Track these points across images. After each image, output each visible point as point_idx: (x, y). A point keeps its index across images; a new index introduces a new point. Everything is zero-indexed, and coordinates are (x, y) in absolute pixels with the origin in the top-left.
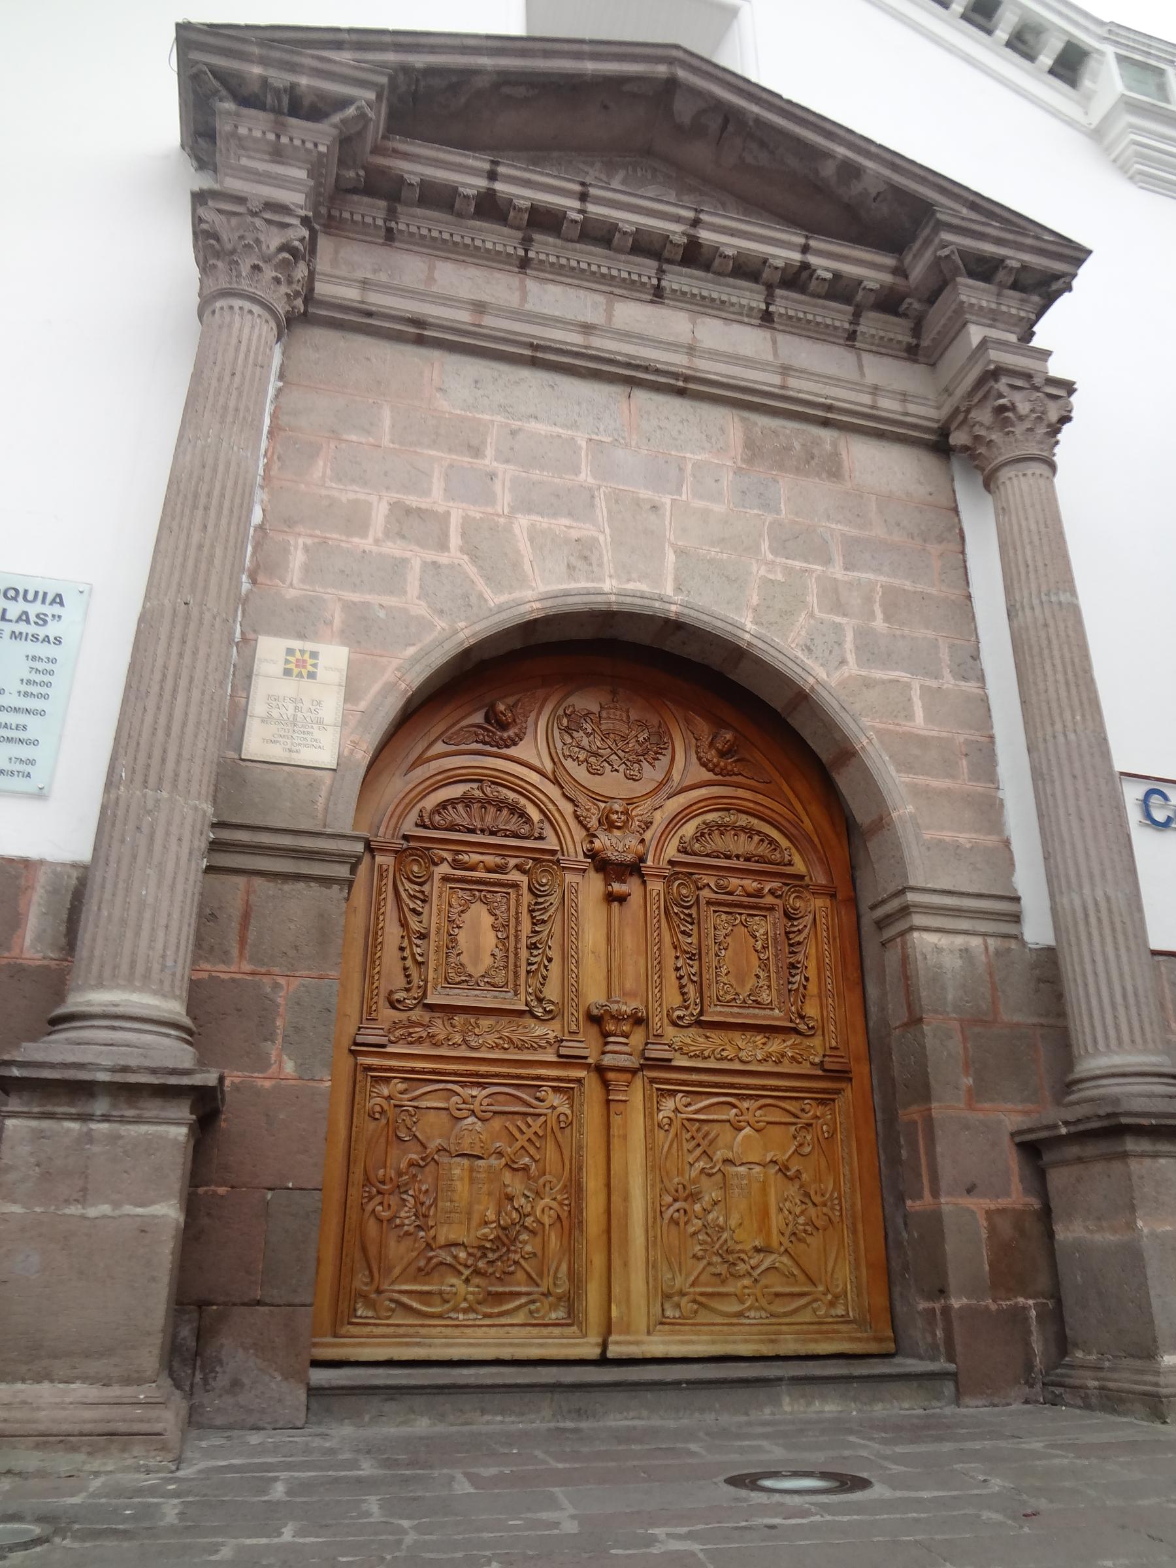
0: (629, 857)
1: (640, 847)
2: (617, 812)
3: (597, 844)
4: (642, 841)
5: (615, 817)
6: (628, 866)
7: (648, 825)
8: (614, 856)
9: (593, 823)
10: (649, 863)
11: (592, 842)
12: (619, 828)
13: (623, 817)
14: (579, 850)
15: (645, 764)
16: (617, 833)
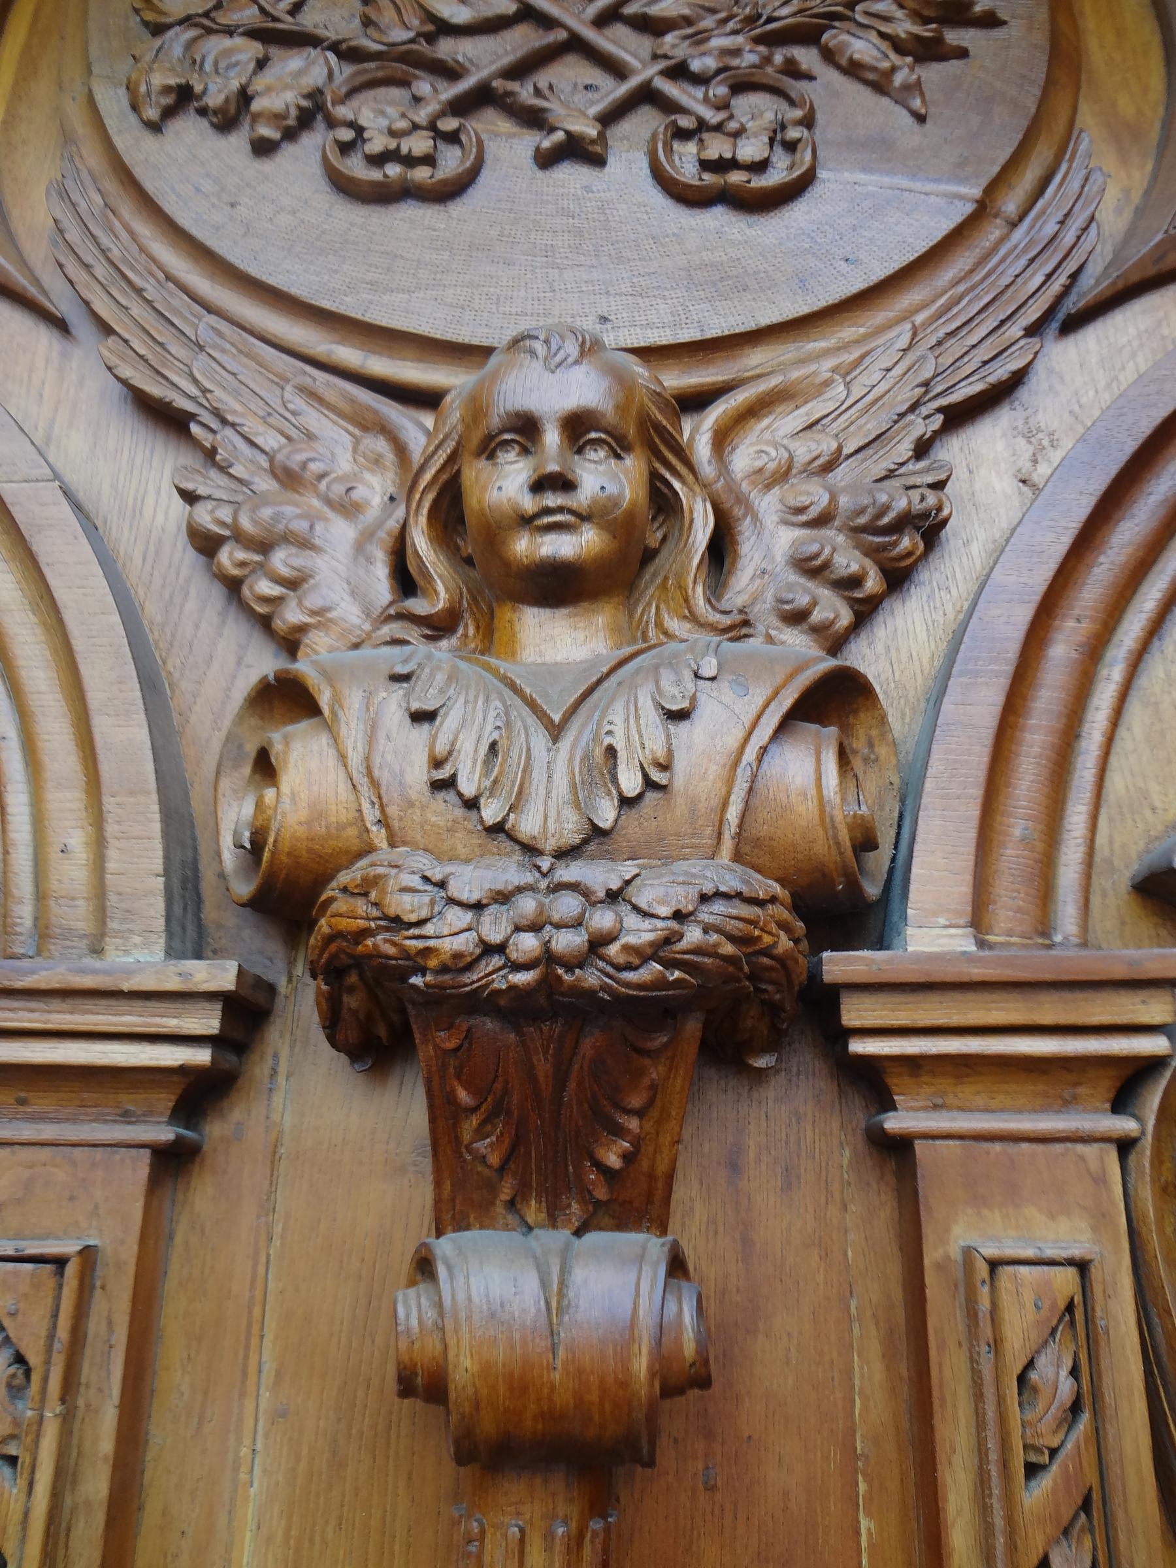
0: (668, 901)
1: (804, 773)
2: (526, 428)
3: (314, 782)
4: (834, 700)
5: (506, 483)
6: (640, 1016)
7: (903, 545)
8: (448, 903)
9: (342, 581)
10: (932, 932)
11: (265, 767)
12: (558, 586)
13: (604, 478)
14: (140, 863)
15: (828, 88)
16: (559, 642)
